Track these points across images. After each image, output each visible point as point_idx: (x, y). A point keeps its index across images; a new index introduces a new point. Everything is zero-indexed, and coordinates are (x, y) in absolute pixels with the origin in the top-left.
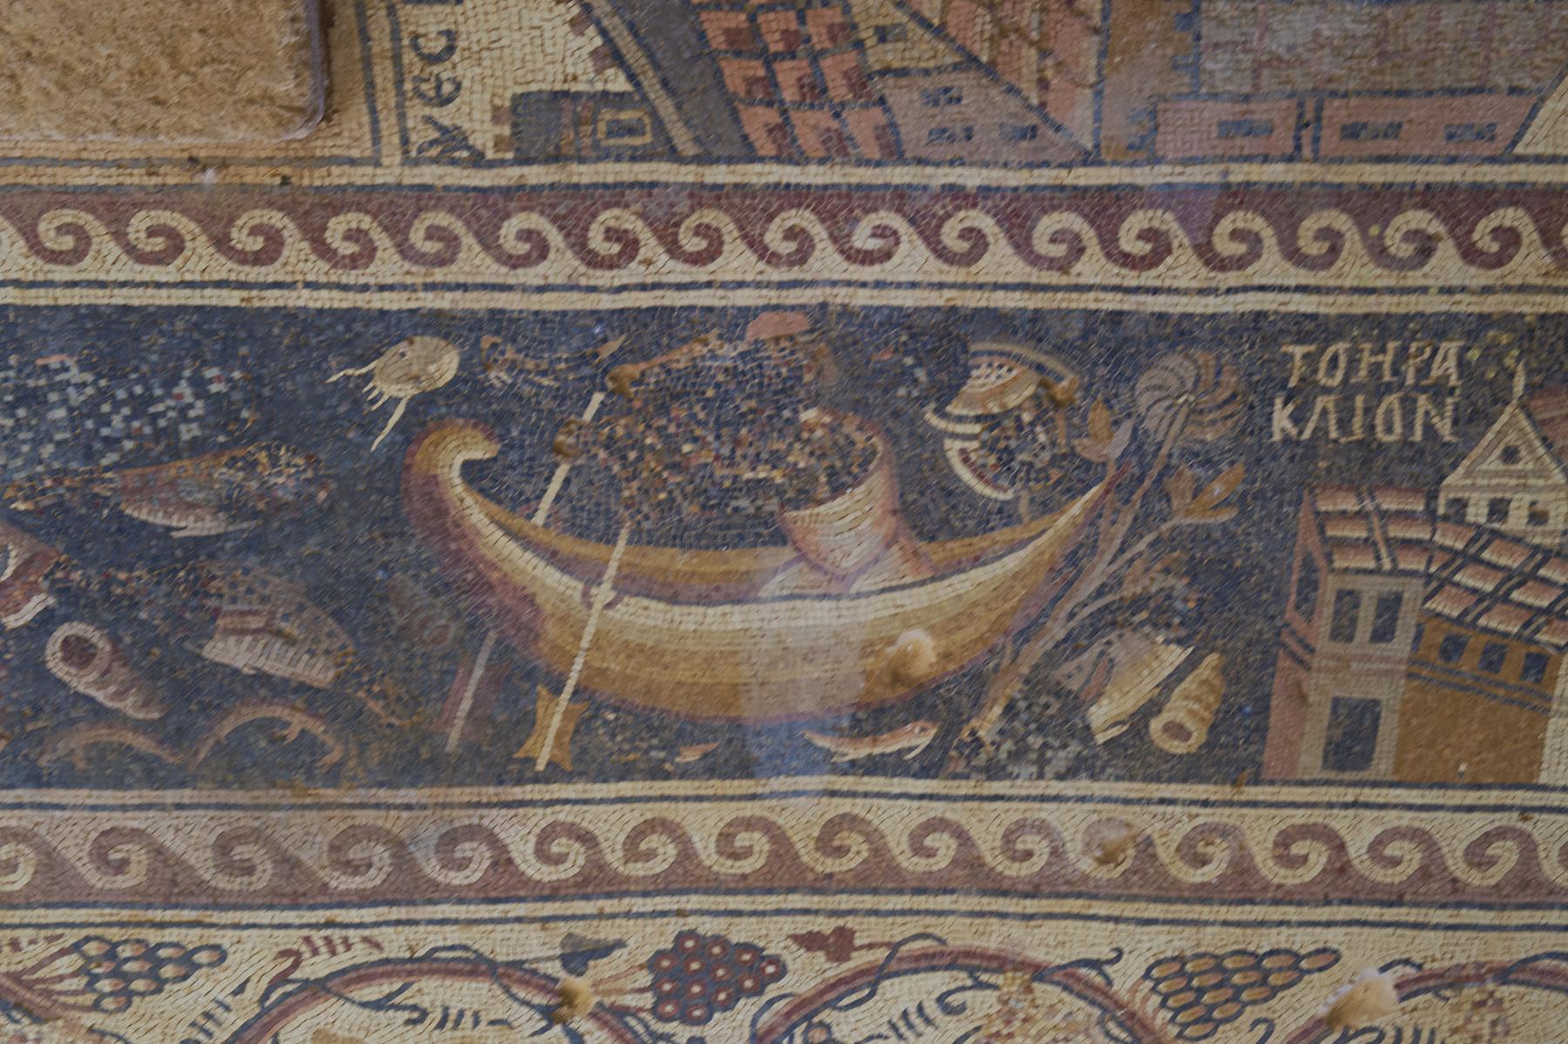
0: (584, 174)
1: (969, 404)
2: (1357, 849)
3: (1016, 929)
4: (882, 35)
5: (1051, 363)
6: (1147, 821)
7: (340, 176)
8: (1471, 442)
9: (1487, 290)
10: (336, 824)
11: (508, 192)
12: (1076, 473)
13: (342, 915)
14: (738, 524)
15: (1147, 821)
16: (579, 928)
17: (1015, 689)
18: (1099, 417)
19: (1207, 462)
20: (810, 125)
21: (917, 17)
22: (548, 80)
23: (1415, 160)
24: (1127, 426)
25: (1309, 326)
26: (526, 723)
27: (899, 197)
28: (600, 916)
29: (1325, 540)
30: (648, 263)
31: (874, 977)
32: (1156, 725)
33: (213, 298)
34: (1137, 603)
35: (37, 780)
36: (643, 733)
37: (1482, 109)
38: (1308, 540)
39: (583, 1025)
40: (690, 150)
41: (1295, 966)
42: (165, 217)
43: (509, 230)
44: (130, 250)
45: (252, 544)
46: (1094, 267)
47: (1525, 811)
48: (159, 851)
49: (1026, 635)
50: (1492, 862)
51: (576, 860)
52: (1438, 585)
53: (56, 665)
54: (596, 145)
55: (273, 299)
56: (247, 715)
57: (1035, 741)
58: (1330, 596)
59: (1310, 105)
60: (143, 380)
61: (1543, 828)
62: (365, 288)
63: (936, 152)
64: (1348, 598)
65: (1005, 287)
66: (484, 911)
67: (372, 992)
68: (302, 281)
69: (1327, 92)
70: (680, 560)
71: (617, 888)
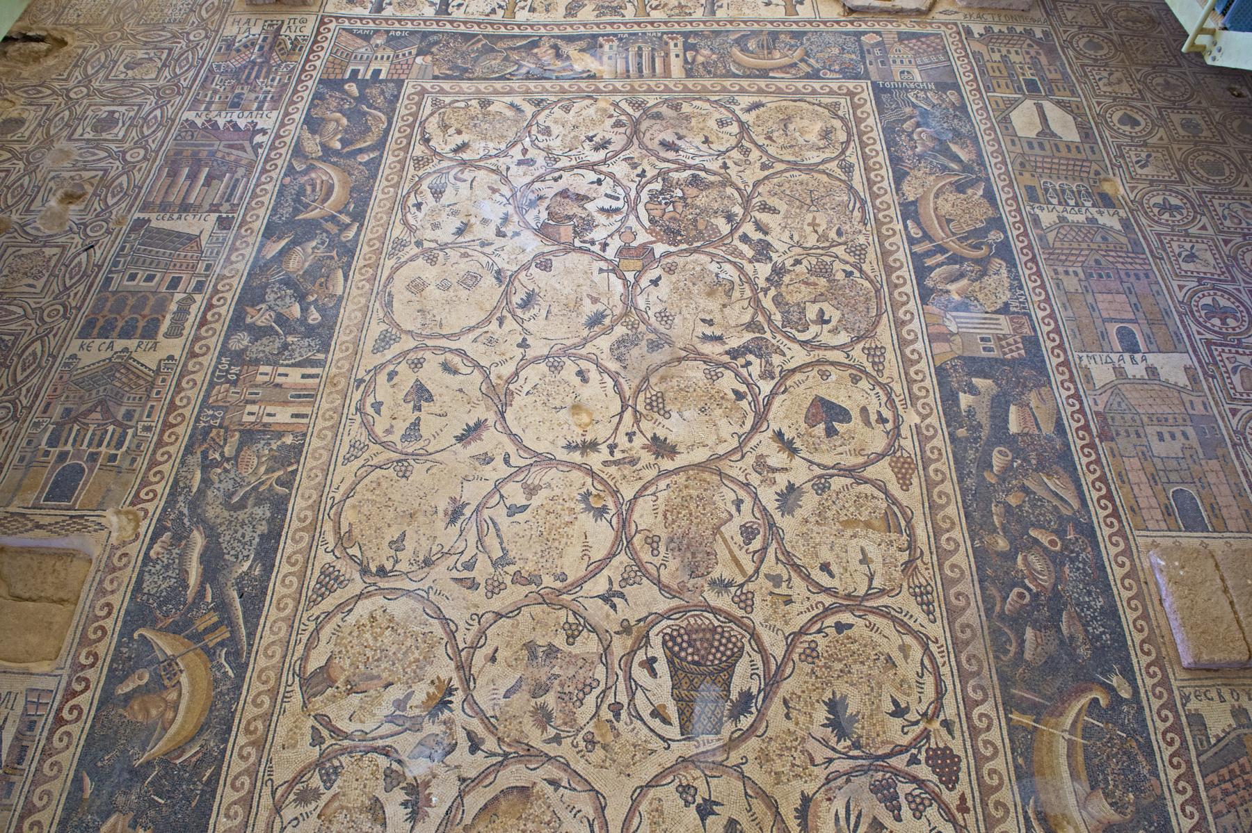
10: (982, 656)
13: (952, 656)
16: (957, 725)
26: (1024, 712)
28: (962, 732)
33: (1129, 638)
35: (980, 581)
36: (1025, 747)
39: (922, 725)
42: (1146, 629)
45: (1062, 642)
48: (964, 609)
51: (982, 725)
53: (1016, 590)
55: (1132, 652)
56: (1012, 636)
67: (926, 662)
68: (1139, 661)
70: (1080, 758)
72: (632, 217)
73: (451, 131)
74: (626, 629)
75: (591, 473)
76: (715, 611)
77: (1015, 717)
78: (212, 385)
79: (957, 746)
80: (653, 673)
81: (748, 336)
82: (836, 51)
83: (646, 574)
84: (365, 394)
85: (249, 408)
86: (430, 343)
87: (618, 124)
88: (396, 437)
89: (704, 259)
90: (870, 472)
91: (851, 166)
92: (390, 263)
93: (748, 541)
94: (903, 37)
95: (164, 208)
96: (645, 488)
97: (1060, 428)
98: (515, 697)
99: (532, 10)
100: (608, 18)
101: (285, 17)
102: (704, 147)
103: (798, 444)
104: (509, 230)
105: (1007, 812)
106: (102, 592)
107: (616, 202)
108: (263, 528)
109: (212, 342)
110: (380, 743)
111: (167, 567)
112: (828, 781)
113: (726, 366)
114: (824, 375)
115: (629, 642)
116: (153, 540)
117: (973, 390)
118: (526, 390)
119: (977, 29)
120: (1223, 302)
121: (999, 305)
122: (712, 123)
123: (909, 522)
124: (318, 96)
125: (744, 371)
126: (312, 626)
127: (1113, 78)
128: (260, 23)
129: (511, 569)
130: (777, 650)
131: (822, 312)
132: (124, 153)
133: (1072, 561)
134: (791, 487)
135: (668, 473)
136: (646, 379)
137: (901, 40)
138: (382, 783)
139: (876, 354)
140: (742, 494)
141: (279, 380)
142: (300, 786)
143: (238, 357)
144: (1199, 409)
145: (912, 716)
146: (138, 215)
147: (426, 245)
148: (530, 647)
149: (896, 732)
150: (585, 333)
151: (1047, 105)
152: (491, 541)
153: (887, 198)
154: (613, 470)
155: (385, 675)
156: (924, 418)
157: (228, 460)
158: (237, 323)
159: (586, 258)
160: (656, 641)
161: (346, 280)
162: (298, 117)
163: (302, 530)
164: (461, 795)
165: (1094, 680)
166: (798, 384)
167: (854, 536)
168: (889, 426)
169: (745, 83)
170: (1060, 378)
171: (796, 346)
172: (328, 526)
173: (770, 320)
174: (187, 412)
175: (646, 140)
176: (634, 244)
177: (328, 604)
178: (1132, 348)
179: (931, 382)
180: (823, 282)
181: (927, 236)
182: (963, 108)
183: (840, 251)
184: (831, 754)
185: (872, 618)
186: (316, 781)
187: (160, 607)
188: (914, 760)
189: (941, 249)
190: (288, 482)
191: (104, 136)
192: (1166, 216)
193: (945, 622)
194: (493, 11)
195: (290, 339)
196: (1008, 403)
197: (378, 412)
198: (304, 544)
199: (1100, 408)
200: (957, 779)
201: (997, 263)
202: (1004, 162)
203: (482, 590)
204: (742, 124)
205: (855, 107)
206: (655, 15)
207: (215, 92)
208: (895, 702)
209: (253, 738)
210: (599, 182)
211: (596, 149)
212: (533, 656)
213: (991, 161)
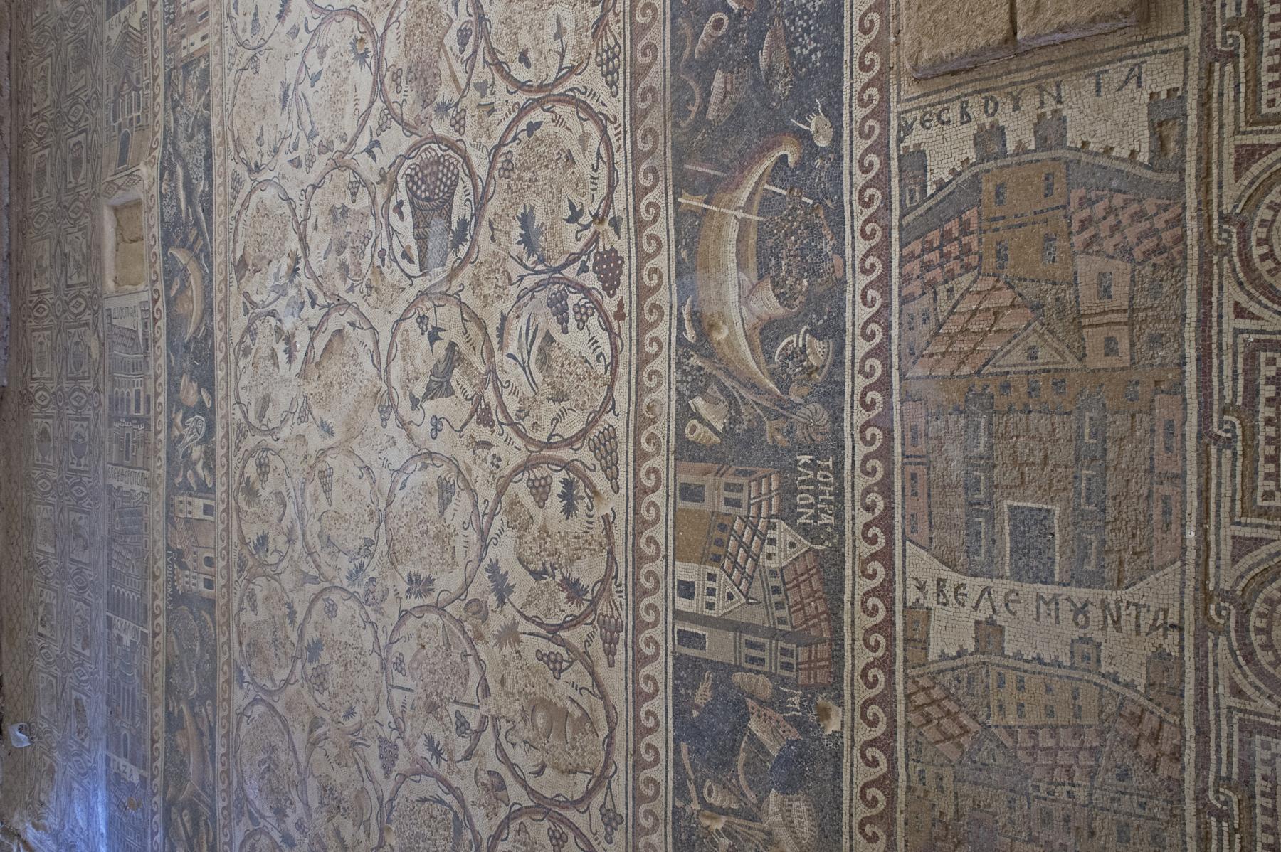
0: (895, 183)
1: (810, 342)
2: (653, 497)
3: (625, 378)
4: (950, 290)
5: (825, 370)
7: (893, 89)
9: (854, 533)
11: (888, 154)
12: (784, 385)
13: (628, 136)
14: (765, 264)
15: (662, 421)
16: (624, 222)
17: (707, 370)
18: (805, 390)
19: (789, 432)
20: (915, 267)
21: (958, 302)
23: (903, 503)
24: (802, 401)
25: (840, 466)
26: (695, 192)
27: (887, 305)
29: (761, 478)
30: (861, 213)
31: (609, 329)
32: (695, 422)
34: (738, 411)
35: (674, 18)
37: (923, 527)
40: (904, 222)
41: (613, 478)
43: (874, 158)
44: (865, 15)
45: (757, 81)
46: (861, 382)
47: (666, 557)
48: (650, 67)
49: (728, 373)
50: (648, 546)
52: (745, 521)
54: (906, 186)
55: (847, 72)
56: (696, 90)
57: (689, 378)
58: (740, 482)
59: (924, 460)
60: (816, 29)
62: (851, 106)
63: (904, 317)
64: (740, 488)
65: (853, 350)
66: (630, 186)
67: (603, 151)
68: (853, 81)
69: (929, 466)
70: (752, 242)
71: (638, 234)
112: (519, 298)
164: (312, 341)
165: (785, 129)
184: (523, 271)
188: (584, 269)
193: (628, 91)
200: (619, 283)
212: (336, 219)
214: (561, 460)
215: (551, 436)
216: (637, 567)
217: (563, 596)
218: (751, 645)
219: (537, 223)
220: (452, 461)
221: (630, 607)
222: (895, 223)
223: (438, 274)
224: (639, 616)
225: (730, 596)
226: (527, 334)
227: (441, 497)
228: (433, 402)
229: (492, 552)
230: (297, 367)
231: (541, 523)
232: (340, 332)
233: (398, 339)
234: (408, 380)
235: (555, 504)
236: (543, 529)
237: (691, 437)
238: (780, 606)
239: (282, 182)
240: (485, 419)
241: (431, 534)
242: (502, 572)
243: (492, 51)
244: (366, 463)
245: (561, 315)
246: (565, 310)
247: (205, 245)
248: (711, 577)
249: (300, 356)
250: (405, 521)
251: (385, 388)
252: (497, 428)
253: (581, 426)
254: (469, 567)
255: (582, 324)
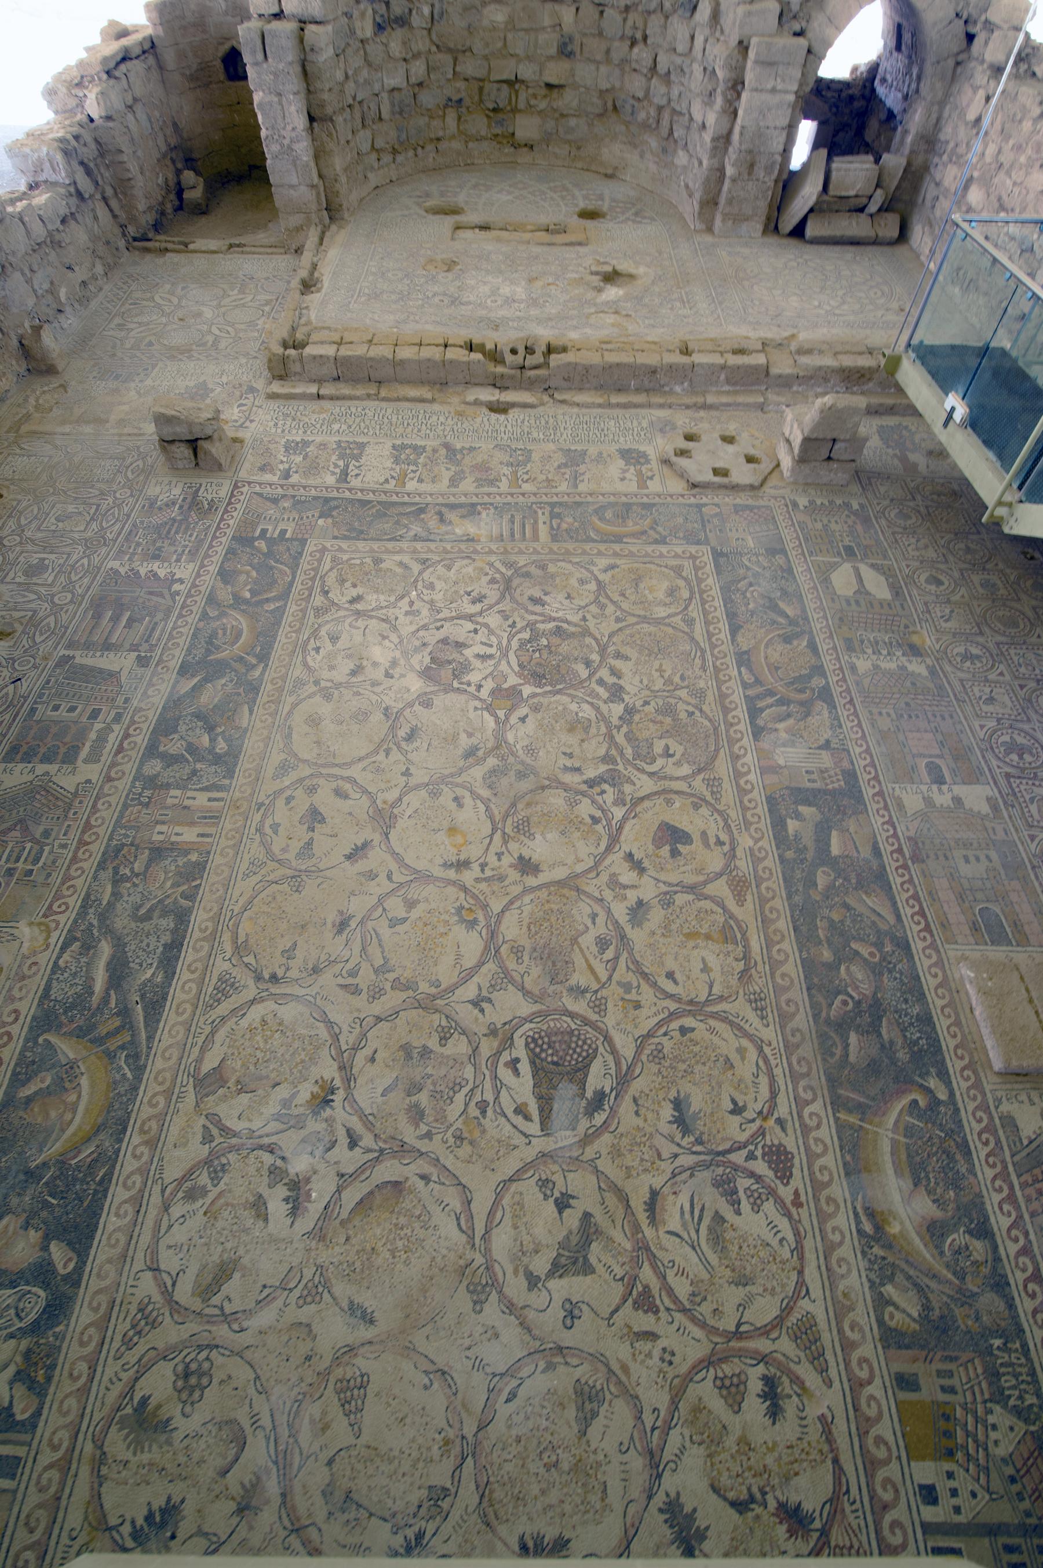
0: (1001, 1133)
2: (870, 1390)
3: (814, 1264)
6: (860, 1309)
8: (1010, 1412)
12: (961, 1275)
14: (917, 1173)
15: (860, 1309)
17: (890, 1259)
20: (1031, 1191)
22: (1021, 1125)
26: (850, 1111)
27: (1020, 1217)
31: (788, 1215)
32: (891, 1309)
38: (964, 1357)
39: (758, 1123)
41: (823, 1370)
45: (883, 1046)
46: (1020, 1277)
47: (899, 1458)
48: (794, 1015)
51: (812, 1123)
52: (964, 1407)
53: (840, 997)
61: (894, 1465)
64: (950, 1374)
68: (954, 1066)
72: (504, 662)
73: (348, 584)
74: (493, 1032)
75: (465, 889)
76: (572, 1015)
77: (842, 1116)
78: (125, 806)
79: (790, 1143)
80: (516, 1072)
81: (603, 768)
82: (680, 520)
83: (512, 981)
84: (264, 816)
85: (159, 828)
86: (324, 771)
87: (493, 581)
88: (291, 856)
89: (565, 699)
90: (710, 889)
91: (693, 620)
92: (291, 699)
93: (602, 951)
94: (737, 509)
95: (88, 646)
96: (511, 902)
97: (876, 851)
98: (392, 1095)
99: (420, 481)
100: (486, 489)
101: (204, 481)
102: (566, 602)
103: (646, 864)
104: (396, 672)
105: (838, 1207)
106: (11, 999)
107: (491, 653)
108: (167, 938)
109: (127, 768)
110: (266, 1141)
111: (74, 975)
112: (674, 1175)
113: (583, 794)
114: (669, 802)
115: (496, 1044)
116: (63, 949)
117: (798, 816)
118: (408, 813)
119: (803, 501)
120: (1020, 740)
121: (822, 742)
122: (573, 581)
123: (744, 934)
124: (231, 552)
125: (599, 799)
126: (208, 1029)
127: (921, 544)
128: (180, 485)
129: (391, 976)
130: (627, 1049)
131: (667, 747)
132: (53, 596)
133: (890, 971)
134: (640, 903)
135: (533, 889)
136: (513, 805)
137: (736, 512)
138: (266, 1180)
139: (714, 783)
140: (597, 909)
141: (187, 803)
142: (188, 1184)
143: (151, 782)
144: (1000, 835)
145: (750, 1114)
146: (63, 652)
147: (323, 684)
148: (406, 1049)
149: (734, 1130)
150: (462, 763)
151: (864, 569)
152: (374, 950)
153: (724, 647)
154: (483, 886)
155: (273, 1075)
156: (757, 841)
157: (137, 875)
158: (152, 750)
159: (463, 698)
160: (519, 1042)
161: (251, 712)
162: (213, 569)
163: (204, 939)
164: (339, 1191)
165: (912, 1082)
166: (646, 810)
167: (695, 947)
168: (726, 848)
169: (602, 547)
170: (875, 806)
171: (644, 777)
172: (227, 937)
173: (622, 754)
174: (101, 831)
175: (517, 595)
176: (505, 686)
177: (223, 1008)
178: (940, 781)
179: (762, 809)
180: (668, 720)
181: (758, 682)
182: (790, 571)
183: (683, 693)
184: (676, 1149)
185: (712, 1022)
186: (204, 1179)
187: (65, 1012)
188: (751, 1156)
189: (771, 693)
190: (191, 897)
191: (35, 580)
192: (968, 664)
194: (387, 481)
195: (198, 766)
196: (830, 828)
197: (276, 833)
198: (203, 953)
199: (912, 834)
201: (820, 706)
202: (825, 617)
203: (364, 996)
204: (599, 583)
205: (697, 569)
206: (527, 487)
207: (138, 544)
208: (734, 1102)
209: (146, 1137)
210: (476, 631)
211: (473, 603)
212: (409, 1056)
213: (814, 616)
214: (757, 1352)
215: (739, 1325)
216: (870, 1476)
217: (782, 1530)
218: (1010, 1549)
219: (695, 1107)
220: (599, 1359)
221: (872, 1528)
222: (1008, 1159)
223: (564, 1138)
224: (883, 1539)
225: (974, 1495)
226: (692, 1212)
227: (580, 1408)
228: (564, 1282)
229: (669, 1483)
230: (306, 1222)
231: (738, 1433)
232: (397, 1186)
233: (506, 1201)
234: (520, 1253)
235: (754, 1407)
236: (744, 1441)
237: (892, 1324)
238: (1020, 1496)
239: (319, 1002)
240: (645, 1303)
241: (565, 1466)
242: (688, 1509)
243: (636, 963)
244: (441, 1365)
245: (731, 1195)
246: (735, 1192)
247: (134, 1042)
248: (950, 1475)
249: (314, 1209)
250: (514, 1450)
251: (479, 1260)
252: (663, 1314)
253: (775, 1312)
254: (632, 1509)
255: (756, 1208)
